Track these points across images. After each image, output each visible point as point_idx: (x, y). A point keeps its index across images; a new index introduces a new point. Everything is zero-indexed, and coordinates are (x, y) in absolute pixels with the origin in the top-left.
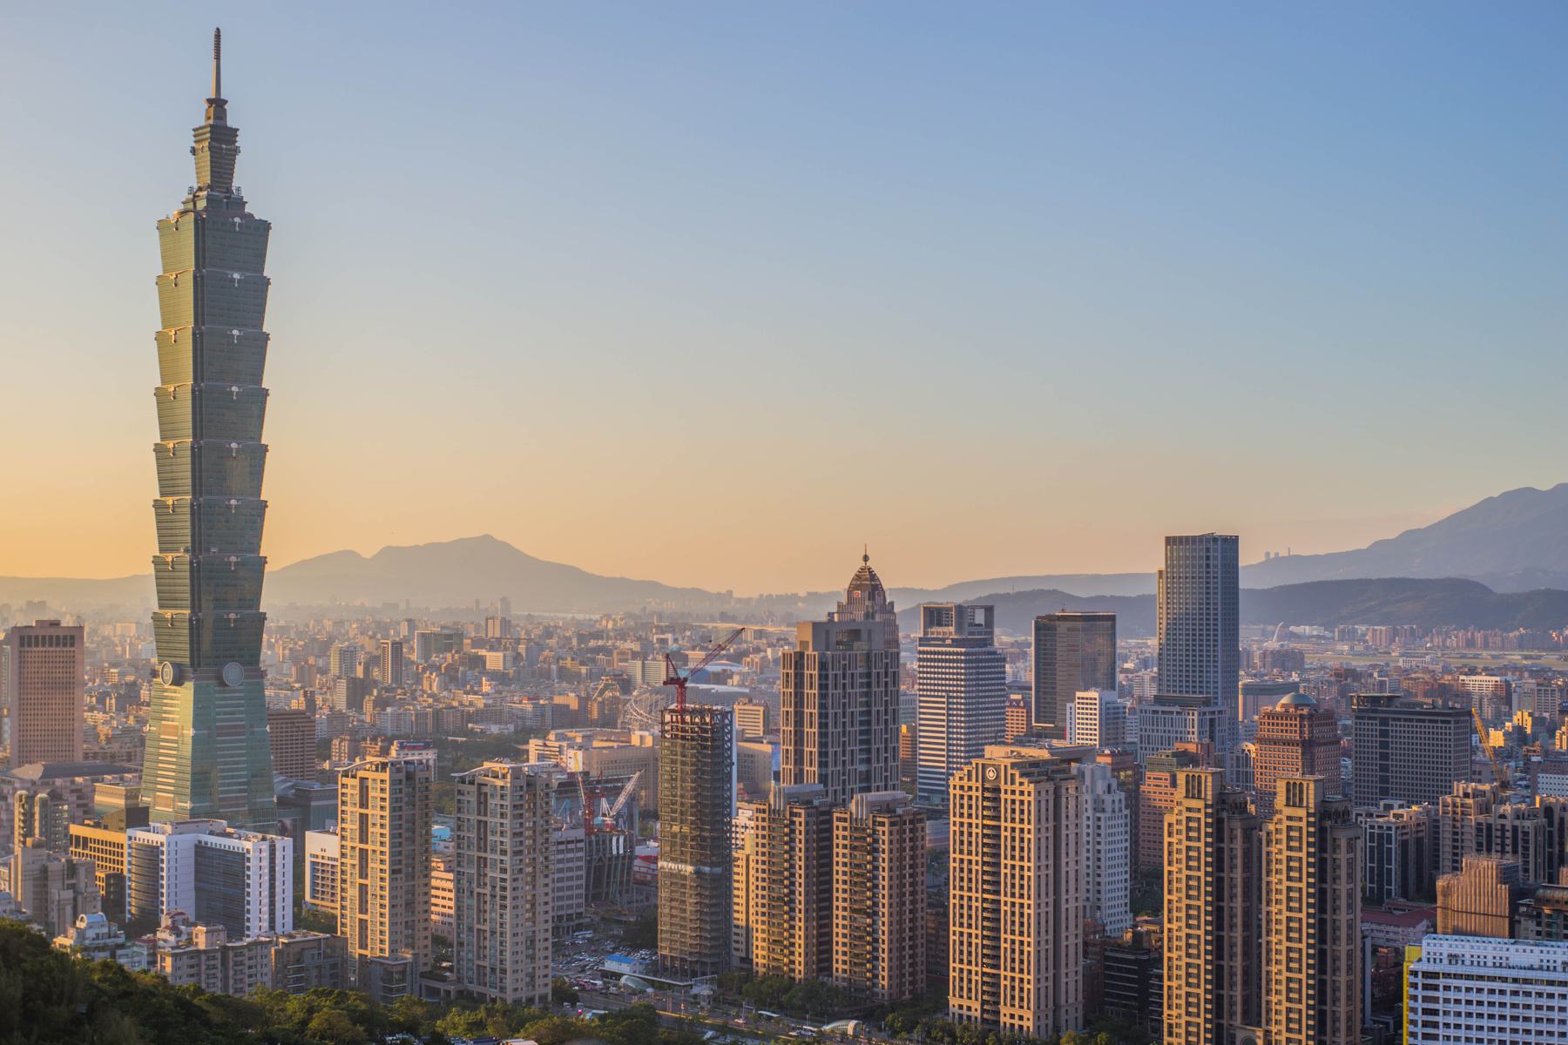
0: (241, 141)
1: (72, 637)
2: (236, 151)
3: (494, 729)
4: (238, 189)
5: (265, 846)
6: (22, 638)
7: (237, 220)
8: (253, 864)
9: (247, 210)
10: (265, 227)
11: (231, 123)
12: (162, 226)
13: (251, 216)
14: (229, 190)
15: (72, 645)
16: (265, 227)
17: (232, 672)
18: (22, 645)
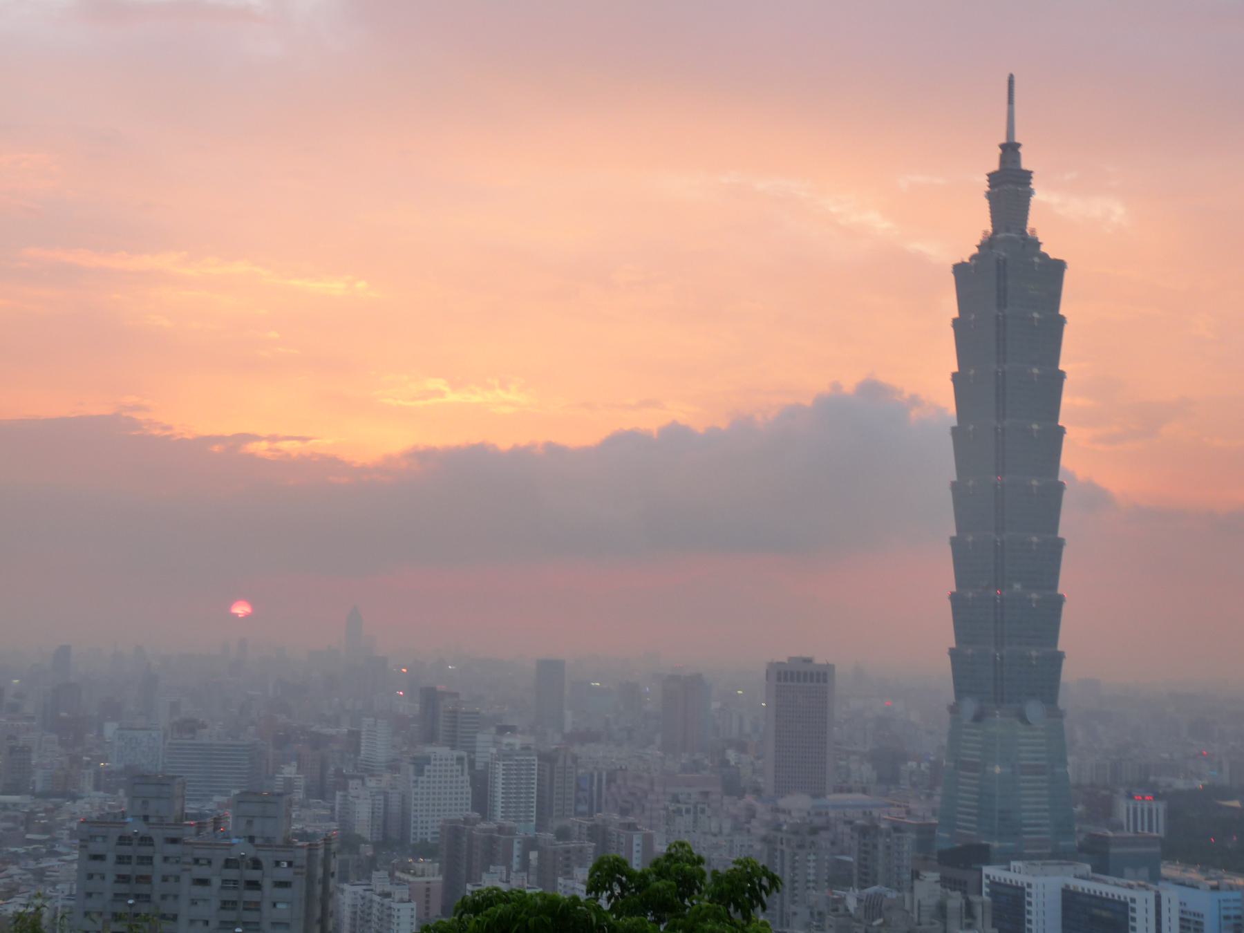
0: (1035, 184)
1: (825, 674)
2: (1030, 193)
3: (1180, 784)
4: (1033, 231)
5: (1151, 896)
6: (779, 673)
7: (1036, 260)
8: (1140, 915)
9: (1043, 249)
10: (1060, 266)
11: (1025, 165)
12: (960, 270)
13: (1045, 256)
14: (1024, 232)
15: (825, 681)
16: (1060, 266)
17: (1034, 709)
18: (779, 679)
